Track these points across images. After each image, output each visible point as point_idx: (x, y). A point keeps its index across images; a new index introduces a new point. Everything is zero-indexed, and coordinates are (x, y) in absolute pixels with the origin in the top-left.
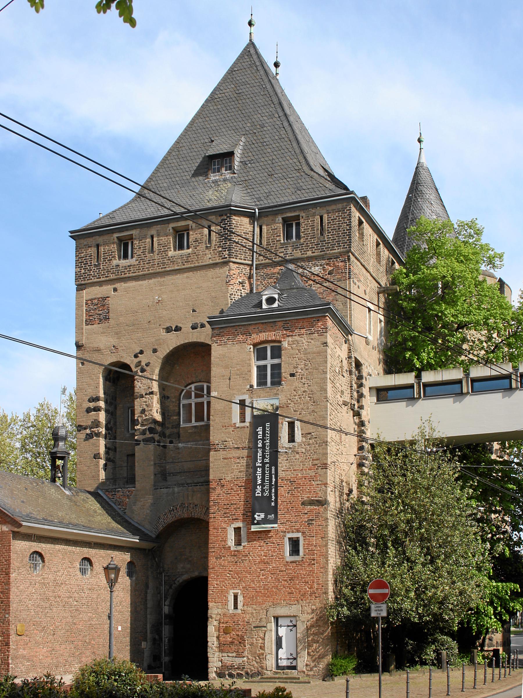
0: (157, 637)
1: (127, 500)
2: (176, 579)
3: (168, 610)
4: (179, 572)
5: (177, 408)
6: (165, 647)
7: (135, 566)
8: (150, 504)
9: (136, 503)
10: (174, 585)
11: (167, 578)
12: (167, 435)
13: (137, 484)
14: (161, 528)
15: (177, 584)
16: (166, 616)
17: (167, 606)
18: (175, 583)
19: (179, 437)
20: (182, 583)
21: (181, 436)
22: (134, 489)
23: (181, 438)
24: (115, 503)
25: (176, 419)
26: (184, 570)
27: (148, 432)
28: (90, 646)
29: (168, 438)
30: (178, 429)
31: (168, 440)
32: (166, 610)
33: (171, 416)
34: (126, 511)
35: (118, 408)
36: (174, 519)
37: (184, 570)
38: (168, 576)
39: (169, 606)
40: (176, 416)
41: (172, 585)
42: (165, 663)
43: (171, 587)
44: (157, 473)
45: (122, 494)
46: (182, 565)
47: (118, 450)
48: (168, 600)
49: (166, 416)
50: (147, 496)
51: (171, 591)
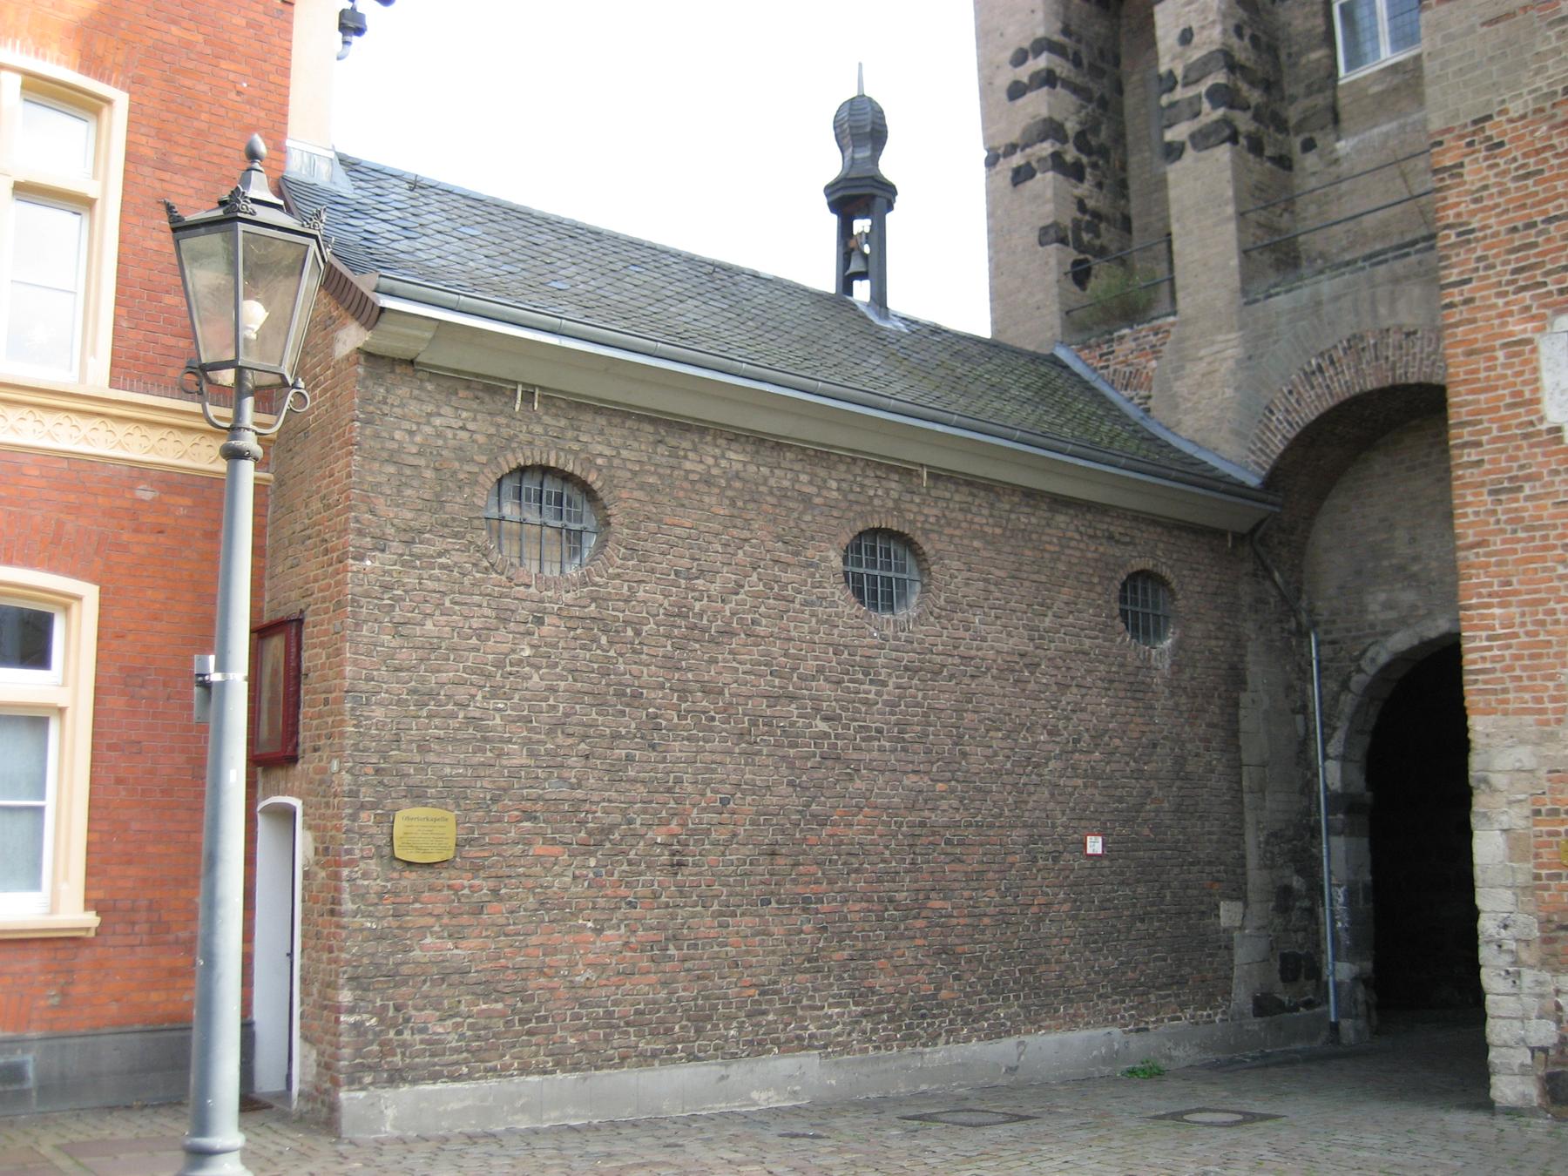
0: (1297, 882)
1: (1154, 364)
2: (1364, 652)
3: (1338, 775)
4: (1372, 626)
5: (1319, 21)
6: (1334, 922)
7: (1172, 593)
8: (1231, 363)
9: (1182, 367)
10: (1356, 678)
11: (1327, 651)
12: (1293, 122)
13: (1183, 302)
14: (1278, 445)
15: (1371, 670)
16: (1334, 801)
17: (1335, 758)
18: (1360, 670)
19: (1336, 120)
20: (1388, 666)
21: (1343, 116)
22: (1171, 319)
23: (1344, 125)
24: (1112, 384)
25: (1319, 60)
26: (1392, 615)
27: (1206, 106)
28: (920, 923)
29: (1297, 134)
30: (1328, 93)
31: (1297, 142)
32: (1331, 775)
33: (1300, 54)
34: (1151, 403)
35: (1128, 89)
36: (1328, 403)
37: (1392, 615)
38: (1333, 642)
39: (1344, 759)
40: (1319, 47)
41: (1349, 677)
42: (1337, 985)
43: (1345, 686)
44: (1250, 246)
45: (1133, 345)
46: (1382, 597)
47: (1135, 224)
48: (1340, 735)
49: (1283, 57)
50: (1221, 338)
51: (1348, 702)
